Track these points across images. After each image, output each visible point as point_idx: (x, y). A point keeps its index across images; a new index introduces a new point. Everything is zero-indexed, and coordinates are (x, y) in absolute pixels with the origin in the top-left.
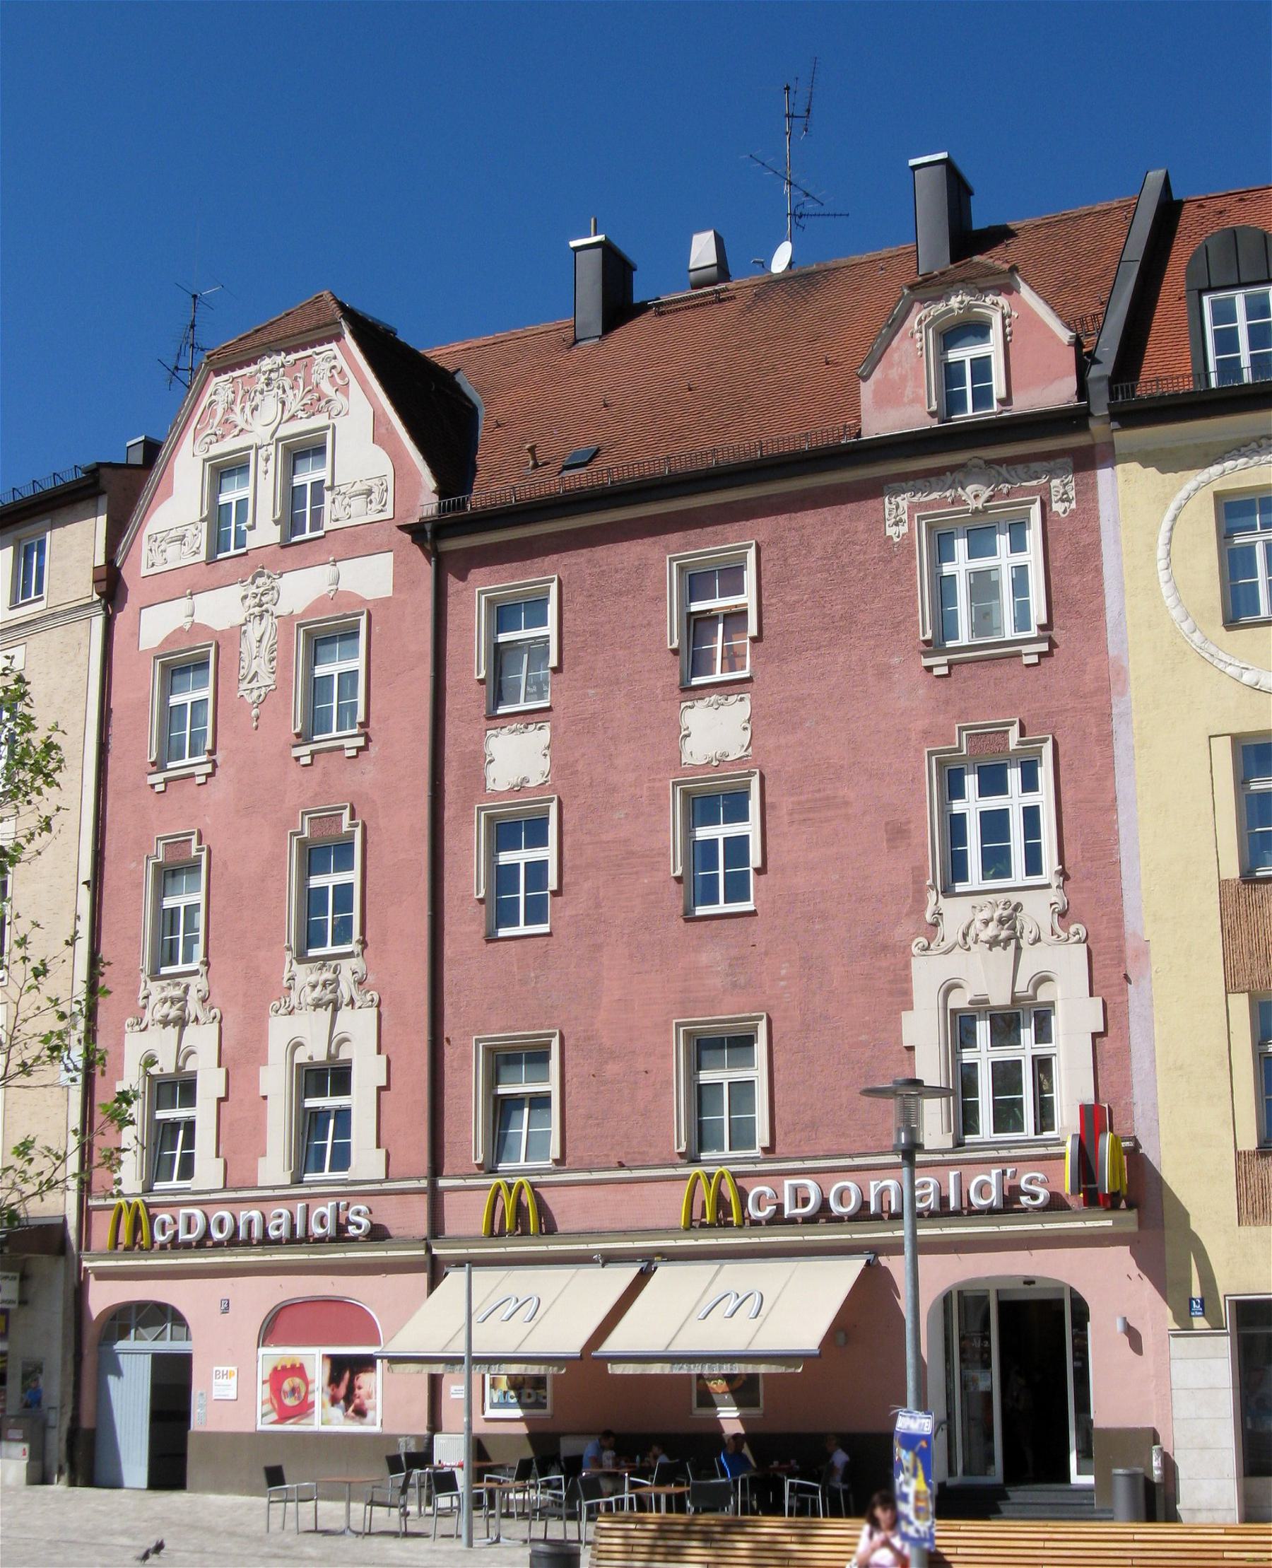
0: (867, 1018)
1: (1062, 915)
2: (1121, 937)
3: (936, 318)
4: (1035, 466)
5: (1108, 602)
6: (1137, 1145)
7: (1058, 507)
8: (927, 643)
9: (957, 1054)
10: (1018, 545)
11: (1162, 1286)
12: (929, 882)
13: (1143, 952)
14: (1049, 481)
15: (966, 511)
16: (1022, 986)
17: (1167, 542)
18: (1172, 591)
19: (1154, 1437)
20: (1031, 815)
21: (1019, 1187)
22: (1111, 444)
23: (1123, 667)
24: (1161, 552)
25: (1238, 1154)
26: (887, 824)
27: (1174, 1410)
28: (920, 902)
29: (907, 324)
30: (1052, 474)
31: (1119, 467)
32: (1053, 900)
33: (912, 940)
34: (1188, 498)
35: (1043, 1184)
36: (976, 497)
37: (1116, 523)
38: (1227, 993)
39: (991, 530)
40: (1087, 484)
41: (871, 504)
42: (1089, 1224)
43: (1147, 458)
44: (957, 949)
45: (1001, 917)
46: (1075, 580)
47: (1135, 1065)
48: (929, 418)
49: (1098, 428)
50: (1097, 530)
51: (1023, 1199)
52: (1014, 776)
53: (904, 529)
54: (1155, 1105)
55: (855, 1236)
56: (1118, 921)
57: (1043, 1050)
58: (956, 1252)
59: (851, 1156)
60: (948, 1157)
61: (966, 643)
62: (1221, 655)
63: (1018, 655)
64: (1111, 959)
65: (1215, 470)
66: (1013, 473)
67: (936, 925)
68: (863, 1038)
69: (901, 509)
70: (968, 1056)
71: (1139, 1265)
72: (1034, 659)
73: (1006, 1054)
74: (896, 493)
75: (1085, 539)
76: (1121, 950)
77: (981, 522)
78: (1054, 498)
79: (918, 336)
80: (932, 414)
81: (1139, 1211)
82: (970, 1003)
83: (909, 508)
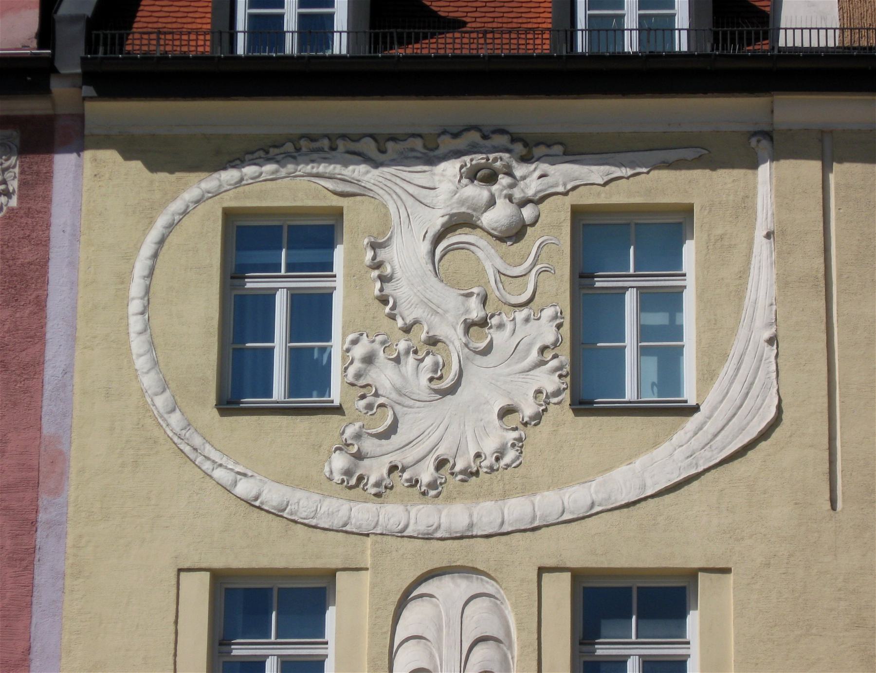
5: (49, 354)
17: (146, 273)
18: (146, 347)
22: (81, 117)
23: (61, 453)
24: (136, 288)
31: (88, 154)
34: (185, 213)
37: (75, 236)
40: (38, 173)
50: (44, 243)
62: (209, 450)
65: (229, 175)
75: (27, 254)
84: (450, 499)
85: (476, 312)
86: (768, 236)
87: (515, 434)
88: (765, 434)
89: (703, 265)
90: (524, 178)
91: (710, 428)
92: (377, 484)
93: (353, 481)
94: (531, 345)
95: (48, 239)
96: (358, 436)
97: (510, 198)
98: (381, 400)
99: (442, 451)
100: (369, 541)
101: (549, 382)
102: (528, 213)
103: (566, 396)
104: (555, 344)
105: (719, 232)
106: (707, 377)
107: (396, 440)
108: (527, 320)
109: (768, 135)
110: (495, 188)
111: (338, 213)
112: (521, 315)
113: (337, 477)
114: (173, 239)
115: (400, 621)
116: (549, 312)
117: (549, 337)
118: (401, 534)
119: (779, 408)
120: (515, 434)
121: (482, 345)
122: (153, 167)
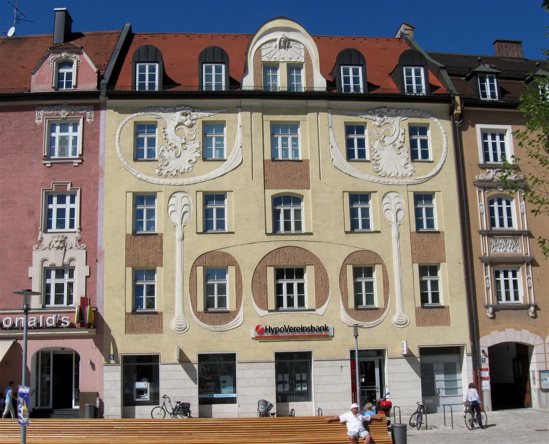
0: (18, 268)
1: (79, 241)
2: (96, 248)
3: (57, 59)
4: (83, 107)
5: (100, 150)
6: (97, 310)
7: (88, 120)
8: (45, 156)
9: (45, 280)
10: (75, 130)
11: (102, 351)
12: (40, 228)
13: (102, 253)
14: (86, 112)
15: (60, 118)
16: (66, 261)
19: (98, 394)
20: (72, 211)
21: (61, 320)
24: (117, 137)
25: (126, 313)
26: (28, 210)
27: (104, 387)
28: (37, 234)
29: (48, 59)
30: (87, 110)
31: (107, 111)
32: (77, 236)
33: (33, 245)
34: (126, 122)
35: (68, 320)
36: (64, 114)
37: (105, 127)
38: (126, 267)
39: (67, 125)
40: (97, 114)
41: (32, 112)
42: (81, 332)
43: (116, 109)
44: (47, 249)
45: (61, 240)
46: (91, 142)
47: (98, 286)
48: (52, 89)
49: (102, 98)
50: (99, 128)
51: (62, 324)
52: (68, 199)
53: (41, 121)
54: (103, 298)
55: (10, 334)
56: (95, 244)
57: (71, 280)
58: (41, 339)
59: (10, 310)
60: (40, 311)
61: (57, 157)
62: (132, 169)
63: (72, 163)
64: (93, 255)
65: (135, 115)
66: (76, 109)
67: (41, 241)
68: (17, 274)
69: (40, 116)
70: (48, 281)
71: (96, 344)
72: (77, 164)
73: (60, 281)
74: (40, 110)
75: (95, 130)
76: (96, 252)
77: (64, 122)
78: (87, 117)
79: (51, 63)
80: (53, 88)
81: (96, 329)
82: (50, 265)
83: (43, 115)
84: (179, 178)
85: (184, 142)
86: (240, 127)
87: (191, 165)
88: (239, 165)
89: (228, 132)
90: (193, 115)
91: (229, 164)
92: (165, 175)
93: (160, 174)
94: (194, 148)
95: (100, 127)
96: (161, 166)
97: (190, 119)
98: (165, 159)
99: (177, 169)
100: (163, 186)
101: (198, 155)
102: (194, 122)
104: (199, 148)
105: (231, 126)
106: (229, 154)
107: (168, 166)
108: (194, 143)
109: (240, 107)
110: (187, 117)
111: (157, 122)
112: (192, 142)
113: (157, 174)
114: (124, 127)
116: (198, 141)
117: (198, 147)
118: (169, 185)
119: (242, 160)
120: (191, 165)
121: (185, 148)
122: (120, 113)
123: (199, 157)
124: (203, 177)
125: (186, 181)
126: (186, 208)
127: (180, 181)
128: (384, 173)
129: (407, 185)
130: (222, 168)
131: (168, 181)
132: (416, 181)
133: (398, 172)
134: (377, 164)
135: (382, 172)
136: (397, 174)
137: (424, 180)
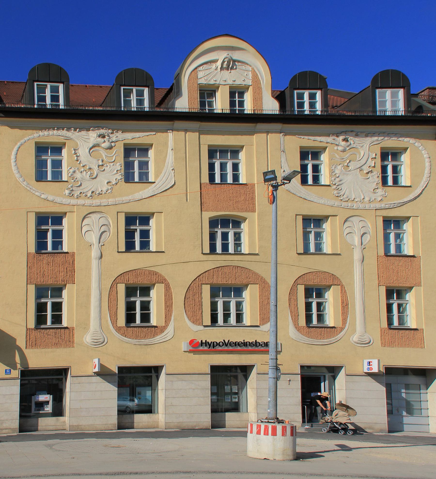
17: (16, 154)
85: (101, 163)
87: (111, 187)
90: (112, 137)
96: (72, 187)
98: (77, 180)
99: (92, 190)
103: (123, 180)
108: (113, 165)
112: (112, 164)
113: (67, 195)
115: (83, 222)
117: (119, 169)
118: (83, 205)
120: (111, 187)
121: (102, 170)
123: (121, 179)
124: (125, 199)
125: (104, 201)
126: (103, 229)
127: (96, 202)
128: (347, 197)
129: (376, 210)
130: (148, 191)
131: (81, 202)
132: (387, 206)
133: (364, 197)
134: (339, 188)
135: (345, 196)
136: (363, 199)
137: (397, 205)
